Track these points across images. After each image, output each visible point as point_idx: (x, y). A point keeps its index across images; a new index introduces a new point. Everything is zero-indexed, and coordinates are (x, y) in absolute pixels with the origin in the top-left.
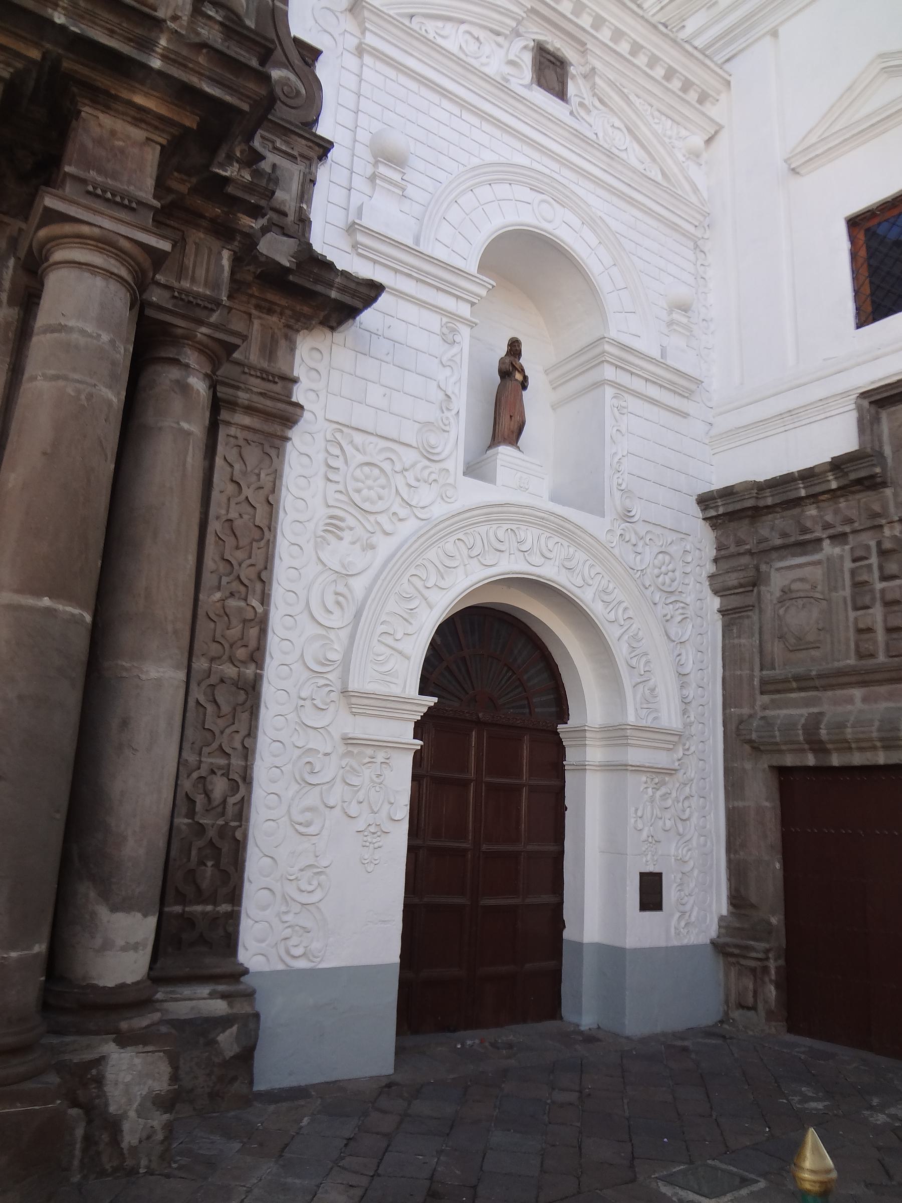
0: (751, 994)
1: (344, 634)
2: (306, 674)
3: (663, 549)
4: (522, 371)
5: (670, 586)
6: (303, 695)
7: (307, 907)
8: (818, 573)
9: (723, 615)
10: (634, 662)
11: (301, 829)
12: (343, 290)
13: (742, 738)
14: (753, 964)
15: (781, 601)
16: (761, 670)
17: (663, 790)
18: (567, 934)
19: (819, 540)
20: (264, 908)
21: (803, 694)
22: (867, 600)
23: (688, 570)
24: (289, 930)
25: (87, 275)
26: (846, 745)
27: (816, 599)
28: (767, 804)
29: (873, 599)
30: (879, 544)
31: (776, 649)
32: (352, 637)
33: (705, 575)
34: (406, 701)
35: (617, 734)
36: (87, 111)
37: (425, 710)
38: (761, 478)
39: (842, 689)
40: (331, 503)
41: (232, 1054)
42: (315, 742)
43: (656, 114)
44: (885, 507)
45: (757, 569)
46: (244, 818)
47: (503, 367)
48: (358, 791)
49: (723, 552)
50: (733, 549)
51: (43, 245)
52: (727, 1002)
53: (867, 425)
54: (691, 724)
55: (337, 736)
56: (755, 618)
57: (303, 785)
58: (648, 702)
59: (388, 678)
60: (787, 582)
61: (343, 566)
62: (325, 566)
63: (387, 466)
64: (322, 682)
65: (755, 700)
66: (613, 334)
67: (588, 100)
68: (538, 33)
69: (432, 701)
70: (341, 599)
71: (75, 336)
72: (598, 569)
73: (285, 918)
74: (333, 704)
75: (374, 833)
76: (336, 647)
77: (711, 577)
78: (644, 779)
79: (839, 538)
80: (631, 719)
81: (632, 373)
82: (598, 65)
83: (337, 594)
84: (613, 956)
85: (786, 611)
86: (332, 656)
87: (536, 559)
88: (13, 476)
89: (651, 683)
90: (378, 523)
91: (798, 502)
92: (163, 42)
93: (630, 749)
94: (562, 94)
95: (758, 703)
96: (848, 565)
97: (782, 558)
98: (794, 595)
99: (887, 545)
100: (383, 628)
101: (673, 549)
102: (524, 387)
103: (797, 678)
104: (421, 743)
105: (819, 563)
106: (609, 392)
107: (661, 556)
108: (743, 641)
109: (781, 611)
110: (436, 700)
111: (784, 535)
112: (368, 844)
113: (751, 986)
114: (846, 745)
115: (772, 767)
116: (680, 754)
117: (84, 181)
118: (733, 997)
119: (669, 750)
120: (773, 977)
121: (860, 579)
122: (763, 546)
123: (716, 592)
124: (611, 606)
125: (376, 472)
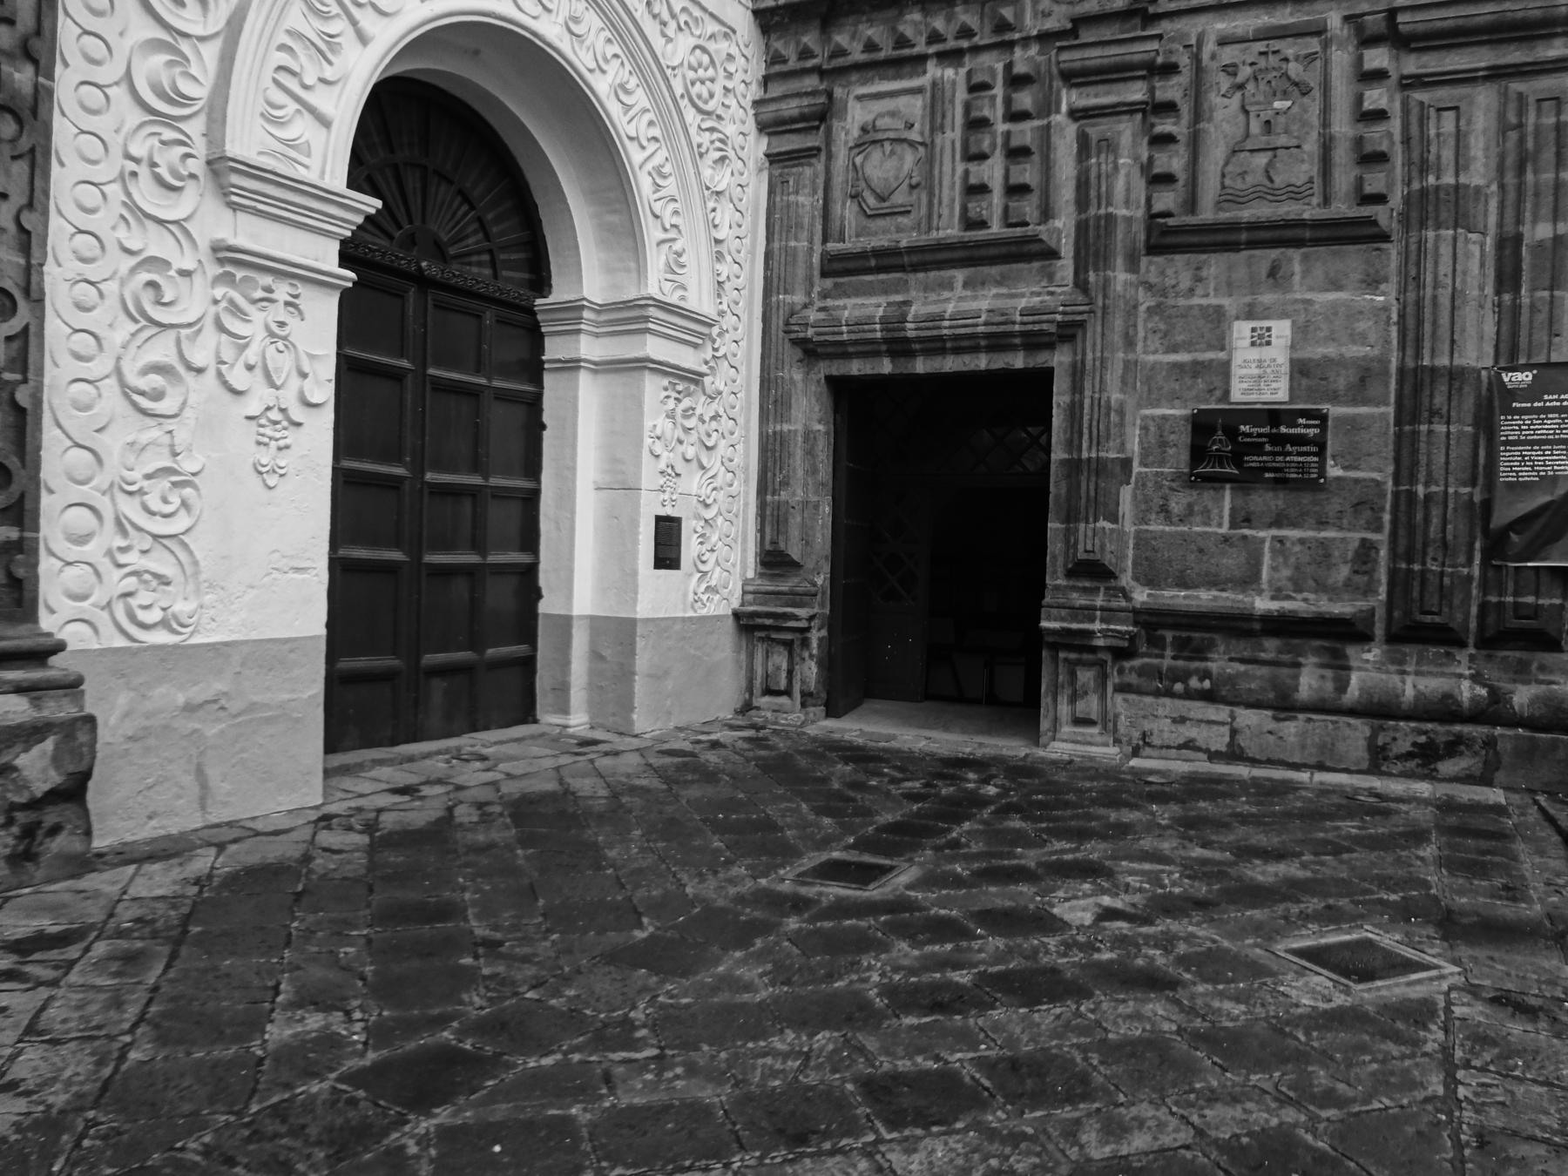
0: (784, 675)
1: (211, 52)
2: (136, 116)
3: (701, 42)
5: (706, 102)
6: (135, 150)
7: (165, 541)
9: (771, 163)
10: (657, 207)
11: (144, 403)
13: (793, 336)
14: (789, 636)
15: (859, 146)
16: (825, 240)
17: (687, 402)
18: (544, 607)
19: (922, 59)
20: (82, 539)
21: (882, 276)
22: (986, 146)
23: (730, 85)
24: (133, 579)
26: (939, 345)
27: (912, 144)
28: (821, 427)
29: (993, 145)
30: (1009, 67)
31: (846, 212)
32: (227, 60)
33: (750, 98)
34: (326, 196)
35: (630, 316)
37: (360, 220)
39: (939, 269)
41: (47, 787)
42: (158, 244)
44: (1019, 15)
45: (830, 95)
46: (31, 367)
48: (246, 346)
49: (777, 68)
50: (793, 64)
52: (750, 689)
54: (721, 313)
55: (204, 245)
56: (820, 167)
57: (144, 323)
58: (674, 273)
59: (293, 154)
64: (168, 134)
65: (812, 285)
69: (373, 204)
72: (616, 49)
73: (122, 559)
74: (191, 184)
75: (276, 423)
76: (194, 70)
77: (756, 103)
78: (665, 382)
79: (951, 57)
80: (653, 290)
84: (618, 635)
85: (865, 158)
86: (186, 87)
89: (677, 246)
93: (649, 338)
95: (817, 289)
96: (961, 95)
97: (864, 83)
98: (880, 136)
99: (1020, 68)
100: (283, 58)
101: (711, 46)
103: (878, 253)
104: (352, 275)
105: (919, 91)
107: (698, 52)
108: (801, 199)
109: (858, 160)
110: (379, 204)
111: (871, 47)
112: (266, 440)
113: (784, 666)
114: (939, 345)
115: (831, 381)
116: (709, 357)
118: (758, 683)
119: (695, 346)
120: (815, 652)
121: (975, 114)
122: (840, 62)
123: (763, 127)
124: (632, 113)
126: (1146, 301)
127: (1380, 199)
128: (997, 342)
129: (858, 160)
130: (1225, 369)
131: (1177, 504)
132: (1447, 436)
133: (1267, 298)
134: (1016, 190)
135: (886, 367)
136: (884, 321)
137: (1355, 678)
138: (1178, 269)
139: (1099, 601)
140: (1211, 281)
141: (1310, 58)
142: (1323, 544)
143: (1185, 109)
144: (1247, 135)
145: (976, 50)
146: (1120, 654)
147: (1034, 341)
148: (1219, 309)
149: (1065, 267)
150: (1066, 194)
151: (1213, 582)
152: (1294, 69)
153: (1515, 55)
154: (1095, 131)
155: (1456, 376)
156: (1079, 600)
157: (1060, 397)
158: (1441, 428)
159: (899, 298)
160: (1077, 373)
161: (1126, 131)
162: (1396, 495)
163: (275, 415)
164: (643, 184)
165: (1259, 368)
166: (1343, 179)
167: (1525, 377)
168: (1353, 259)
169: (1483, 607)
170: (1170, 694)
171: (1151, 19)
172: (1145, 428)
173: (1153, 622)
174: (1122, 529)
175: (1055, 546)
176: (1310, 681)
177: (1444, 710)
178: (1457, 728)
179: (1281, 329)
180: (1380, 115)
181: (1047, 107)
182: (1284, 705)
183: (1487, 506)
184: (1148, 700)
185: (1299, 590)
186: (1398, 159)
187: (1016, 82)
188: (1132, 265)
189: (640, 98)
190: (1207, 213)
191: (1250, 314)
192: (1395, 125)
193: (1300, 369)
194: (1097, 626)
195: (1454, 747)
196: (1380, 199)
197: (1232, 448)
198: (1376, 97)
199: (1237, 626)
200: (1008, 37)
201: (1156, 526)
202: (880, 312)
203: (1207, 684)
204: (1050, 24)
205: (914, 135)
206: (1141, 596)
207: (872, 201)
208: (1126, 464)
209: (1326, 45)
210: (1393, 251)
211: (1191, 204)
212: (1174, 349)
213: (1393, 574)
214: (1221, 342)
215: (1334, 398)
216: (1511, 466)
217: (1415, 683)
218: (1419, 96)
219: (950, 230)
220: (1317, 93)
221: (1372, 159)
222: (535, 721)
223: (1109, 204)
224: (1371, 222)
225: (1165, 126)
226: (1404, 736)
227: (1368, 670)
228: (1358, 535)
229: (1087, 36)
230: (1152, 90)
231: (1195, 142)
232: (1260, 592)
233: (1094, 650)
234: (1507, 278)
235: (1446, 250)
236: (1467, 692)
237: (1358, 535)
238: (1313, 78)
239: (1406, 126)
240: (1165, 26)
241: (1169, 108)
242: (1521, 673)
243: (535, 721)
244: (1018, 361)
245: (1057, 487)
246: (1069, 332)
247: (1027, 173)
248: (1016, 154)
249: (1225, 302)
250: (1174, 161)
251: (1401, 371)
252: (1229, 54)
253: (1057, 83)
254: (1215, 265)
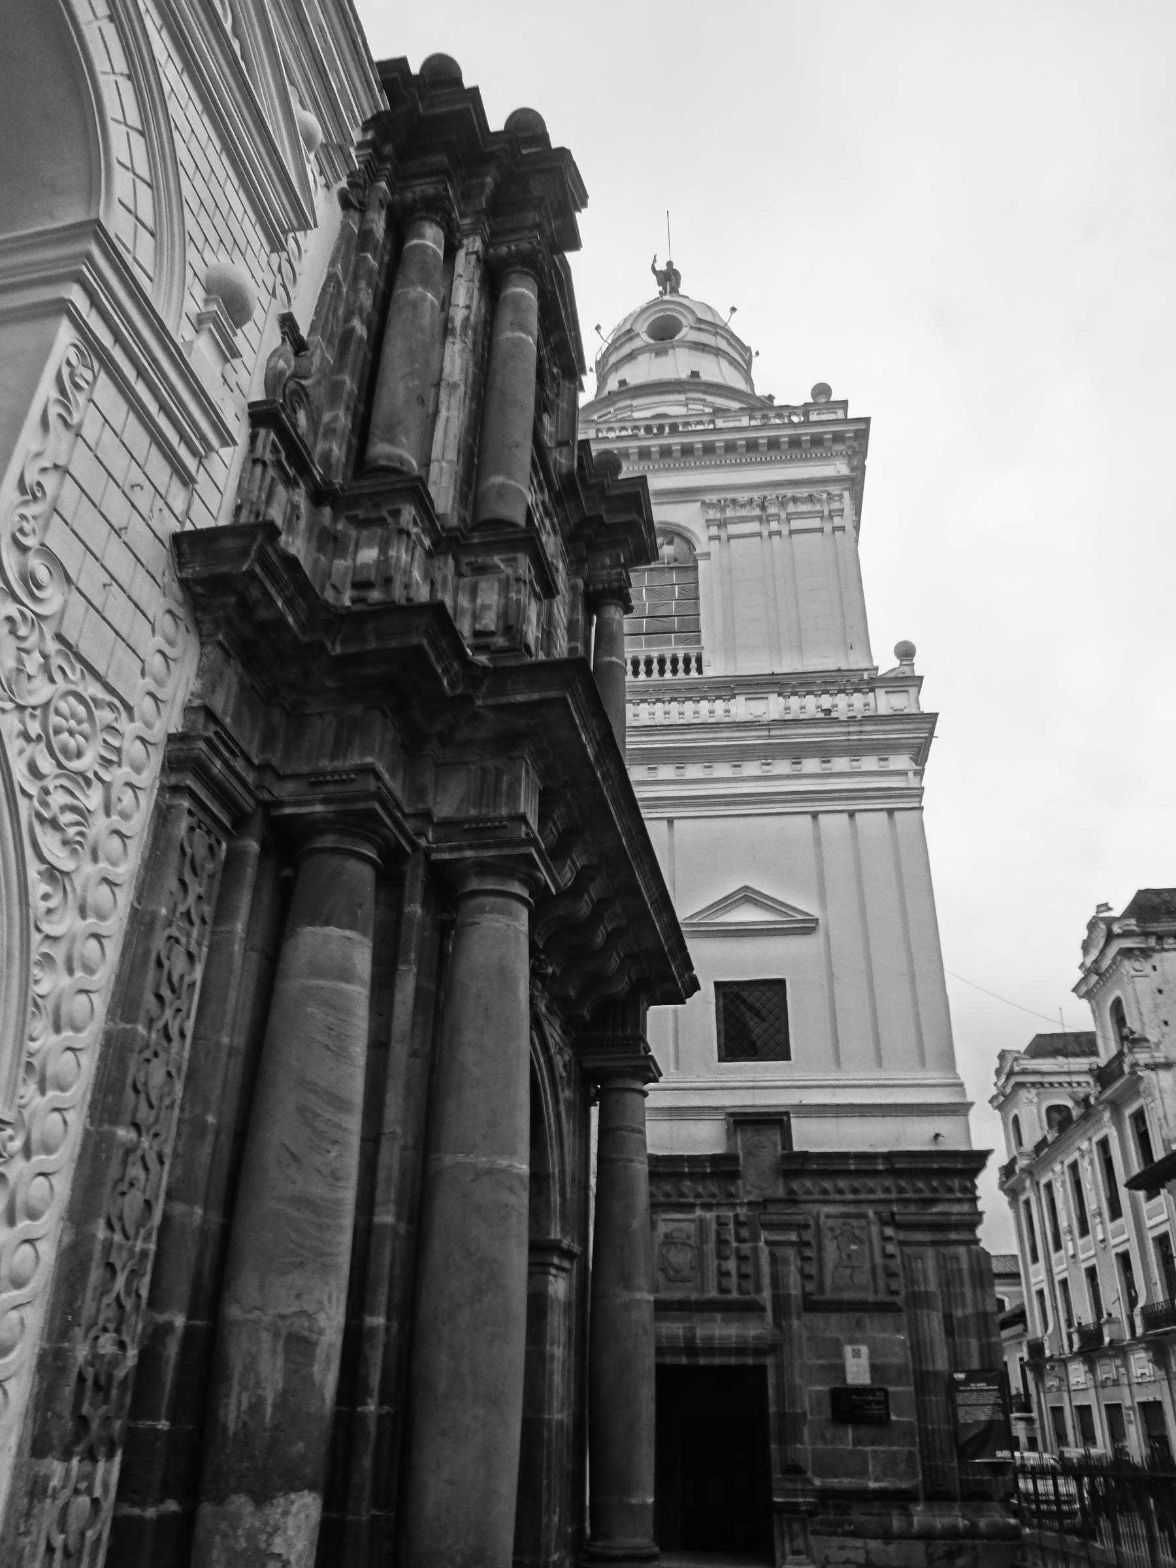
8: (691, 1228)
15: (664, 1244)
22: (728, 1253)
27: (690, 1246)
30: (736, 1216)
38: (660, 1153)
44: (737, 1190)
53: (730, 1134)
60: (669, 1231)
79: (707, 1207)
91: (681, 1176)
96: (714, 1226)
99: (742, 1218)
111: (667, 1195)
126: (805, 1334)
127: (896, 1293)
128: (741, 1351)
129: (664, 1251)
130: (842, 1369)
131: (828, 1434)
132: (936, 1400)
133: (858, 1335)
134: (743, 1276)
135: (684, 1360)
136: (685, 1338)
137: (915, 1520)
138: (818, 1320)
139: (799, 1486)
140: (832, 1326)
141: (862, 1228)
142: (894, 1452)
143: (814, 1243)
144: (841, 1258)
145: (719, 1205)
146: (812, 1513)
147: (758, 1352)
148: (838, 1340)
149: (769, 1314)
150: (766, 1280)
151: (848, 1474)
152: (857, 1232)
153: (939, 1236)
154: (779, 1251)
155: (936, 1374)
156: (790, 1486)
157: (771, 1380)
158: (933, 1398)
159: (687, 1325)
160: (780, 1370)
161: (791, 1253)
162: (920, 1429)
165: (857, 1369)
166: (881, 1284)
167: (960, 1376)
168: (889, 1319)
169: (961, 1481)
170: (835, 1534)
171: (796, 1202)
172: (810, 1397)
173: (824, 1495)
174: (806, 1447)
175: (775, 1457)
176: (896, 1523)
177: (952, 1533)
178: (961, 1542)
179: (864, 1349)
180: (892, 1256)
181: (755, 1238)
182: (887, 1536)
183: (955, 1435)
184: (826, 1538)
185: (885, 1476)
186: (901, 1274)
187: (739, 1224)
188: (799, 1318)
190: (828, 1296)
191: (851, 1341)
192: (899, 1260)
193: (874, 1369)
194: (801, 1500)
195: (960, 1551)
196: (896, 1293)
197: (852, 1407)
198: (891, 1248)
199: (862, 1496)
200: (733, 1201)
201: (820, 1446)
202: (681, 1332)
203: (852, 1527)
204: (752, 1198)
205: (692, 1242)
206: (817, 1482)
207: (672, 1273)
208: (804, 1414)
209: (869, 1223)
210: (904, 1316)
211: (821, 1289)
212: (820, 1357)
213: (923, 1466)
214: (840, 1355)
215: (889, 1383)
216: (964, 1416)
217: (940, 1522)
218: (907, 1250)
219: (713, 1294)
220: (867, 1243)
221: (892, 1275)
223: (788, 1288)
224: (894, 1304)
225: (808, 1253)
226: (940, 1547)
227: (920, 1515)
228: (907, 1449)
229: (771, 1208)
230: (800, 1236)
231: (820, 1261)
232: (869, 1478)
233: (799, 1512)
234: (949, 1331)
235: (925, 1319)
236: (962, 1523)
237: (907, 1449)
238: (865, 1237)
239: (903, 1262)
240: (803, 1206)
241: (807, 1244)
242: (980, 1512)
244: (750, 1361)
245: (773, 1425)
246: (774, 1348)
247: (748, 1269)
248: (742, 1259)
249: (841, 1336)
250: (812, 1269)
251: (915, 1371)
252: (830, 1222)
253: (759, 1227)
254: (834, 1318)
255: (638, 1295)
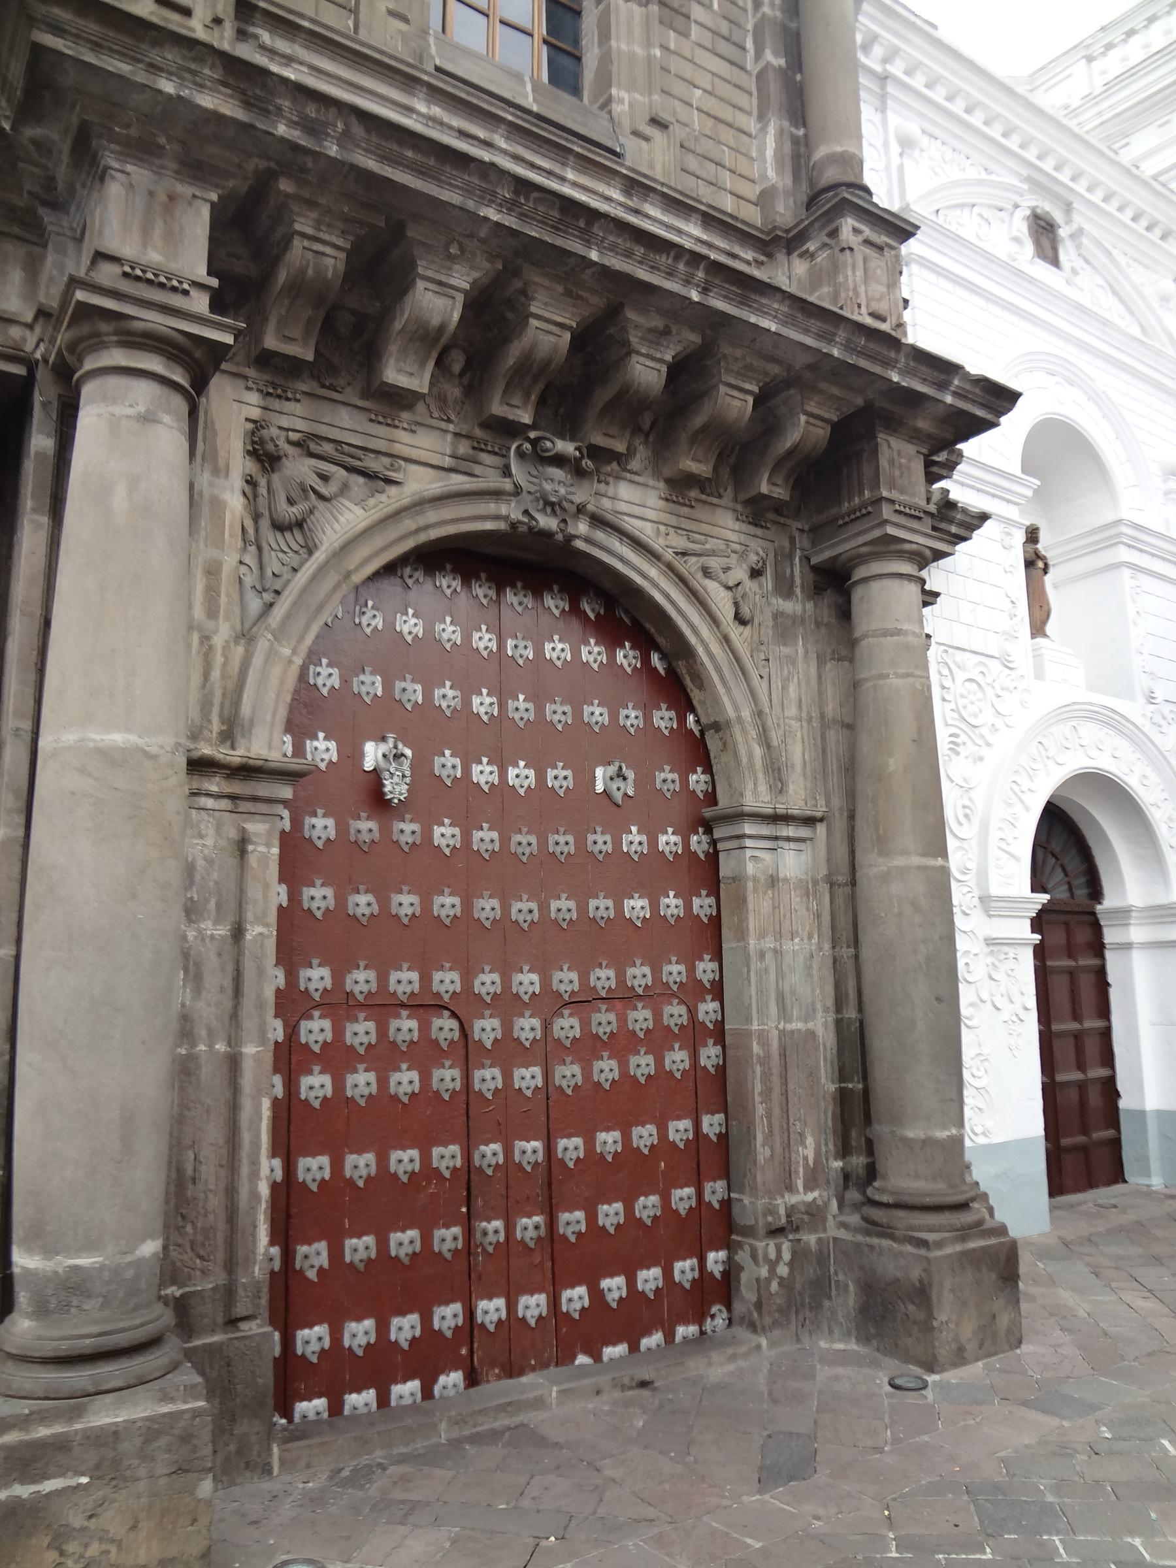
4: (1043, 558)
12: (961, 524)
18: (1123, 1104)
25: (906, 582)
34: (1026, 901)
36: (881, 437)
37: (1040, 907)
40: (950, 722)
43: (1131, 261)
47: (1028, 555)
51: (860, 556)
55: (982, 940)
61: (965, 780)
62: (952, 781)
63: (980, 679)
66: (1126, 515)
67: (1080, 263)
68: (1030, 201)
69: (1044, 898)
70: (968, 811)
71: (910, 638)
72: (1139, 756)
81: (1141, 551)
82: (1087, 226)
83: (964, 807)
87: (1093, 753)
88: (892, 761)
90: (982, 736)
92: (956, 382)
94: (1055, 262)
102: (1046, 573)
106: (1126, 572)
110: (1047, 897)
117: (892, 502)
125: (974, 686)
163: (1015, 1018)
164: (1162, 831)
189: (1154, 778)
222: (1125, 1181)
243: (1125, 1181)
255: (899, 861)
